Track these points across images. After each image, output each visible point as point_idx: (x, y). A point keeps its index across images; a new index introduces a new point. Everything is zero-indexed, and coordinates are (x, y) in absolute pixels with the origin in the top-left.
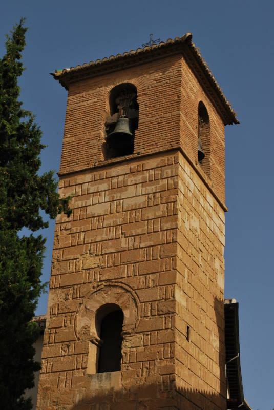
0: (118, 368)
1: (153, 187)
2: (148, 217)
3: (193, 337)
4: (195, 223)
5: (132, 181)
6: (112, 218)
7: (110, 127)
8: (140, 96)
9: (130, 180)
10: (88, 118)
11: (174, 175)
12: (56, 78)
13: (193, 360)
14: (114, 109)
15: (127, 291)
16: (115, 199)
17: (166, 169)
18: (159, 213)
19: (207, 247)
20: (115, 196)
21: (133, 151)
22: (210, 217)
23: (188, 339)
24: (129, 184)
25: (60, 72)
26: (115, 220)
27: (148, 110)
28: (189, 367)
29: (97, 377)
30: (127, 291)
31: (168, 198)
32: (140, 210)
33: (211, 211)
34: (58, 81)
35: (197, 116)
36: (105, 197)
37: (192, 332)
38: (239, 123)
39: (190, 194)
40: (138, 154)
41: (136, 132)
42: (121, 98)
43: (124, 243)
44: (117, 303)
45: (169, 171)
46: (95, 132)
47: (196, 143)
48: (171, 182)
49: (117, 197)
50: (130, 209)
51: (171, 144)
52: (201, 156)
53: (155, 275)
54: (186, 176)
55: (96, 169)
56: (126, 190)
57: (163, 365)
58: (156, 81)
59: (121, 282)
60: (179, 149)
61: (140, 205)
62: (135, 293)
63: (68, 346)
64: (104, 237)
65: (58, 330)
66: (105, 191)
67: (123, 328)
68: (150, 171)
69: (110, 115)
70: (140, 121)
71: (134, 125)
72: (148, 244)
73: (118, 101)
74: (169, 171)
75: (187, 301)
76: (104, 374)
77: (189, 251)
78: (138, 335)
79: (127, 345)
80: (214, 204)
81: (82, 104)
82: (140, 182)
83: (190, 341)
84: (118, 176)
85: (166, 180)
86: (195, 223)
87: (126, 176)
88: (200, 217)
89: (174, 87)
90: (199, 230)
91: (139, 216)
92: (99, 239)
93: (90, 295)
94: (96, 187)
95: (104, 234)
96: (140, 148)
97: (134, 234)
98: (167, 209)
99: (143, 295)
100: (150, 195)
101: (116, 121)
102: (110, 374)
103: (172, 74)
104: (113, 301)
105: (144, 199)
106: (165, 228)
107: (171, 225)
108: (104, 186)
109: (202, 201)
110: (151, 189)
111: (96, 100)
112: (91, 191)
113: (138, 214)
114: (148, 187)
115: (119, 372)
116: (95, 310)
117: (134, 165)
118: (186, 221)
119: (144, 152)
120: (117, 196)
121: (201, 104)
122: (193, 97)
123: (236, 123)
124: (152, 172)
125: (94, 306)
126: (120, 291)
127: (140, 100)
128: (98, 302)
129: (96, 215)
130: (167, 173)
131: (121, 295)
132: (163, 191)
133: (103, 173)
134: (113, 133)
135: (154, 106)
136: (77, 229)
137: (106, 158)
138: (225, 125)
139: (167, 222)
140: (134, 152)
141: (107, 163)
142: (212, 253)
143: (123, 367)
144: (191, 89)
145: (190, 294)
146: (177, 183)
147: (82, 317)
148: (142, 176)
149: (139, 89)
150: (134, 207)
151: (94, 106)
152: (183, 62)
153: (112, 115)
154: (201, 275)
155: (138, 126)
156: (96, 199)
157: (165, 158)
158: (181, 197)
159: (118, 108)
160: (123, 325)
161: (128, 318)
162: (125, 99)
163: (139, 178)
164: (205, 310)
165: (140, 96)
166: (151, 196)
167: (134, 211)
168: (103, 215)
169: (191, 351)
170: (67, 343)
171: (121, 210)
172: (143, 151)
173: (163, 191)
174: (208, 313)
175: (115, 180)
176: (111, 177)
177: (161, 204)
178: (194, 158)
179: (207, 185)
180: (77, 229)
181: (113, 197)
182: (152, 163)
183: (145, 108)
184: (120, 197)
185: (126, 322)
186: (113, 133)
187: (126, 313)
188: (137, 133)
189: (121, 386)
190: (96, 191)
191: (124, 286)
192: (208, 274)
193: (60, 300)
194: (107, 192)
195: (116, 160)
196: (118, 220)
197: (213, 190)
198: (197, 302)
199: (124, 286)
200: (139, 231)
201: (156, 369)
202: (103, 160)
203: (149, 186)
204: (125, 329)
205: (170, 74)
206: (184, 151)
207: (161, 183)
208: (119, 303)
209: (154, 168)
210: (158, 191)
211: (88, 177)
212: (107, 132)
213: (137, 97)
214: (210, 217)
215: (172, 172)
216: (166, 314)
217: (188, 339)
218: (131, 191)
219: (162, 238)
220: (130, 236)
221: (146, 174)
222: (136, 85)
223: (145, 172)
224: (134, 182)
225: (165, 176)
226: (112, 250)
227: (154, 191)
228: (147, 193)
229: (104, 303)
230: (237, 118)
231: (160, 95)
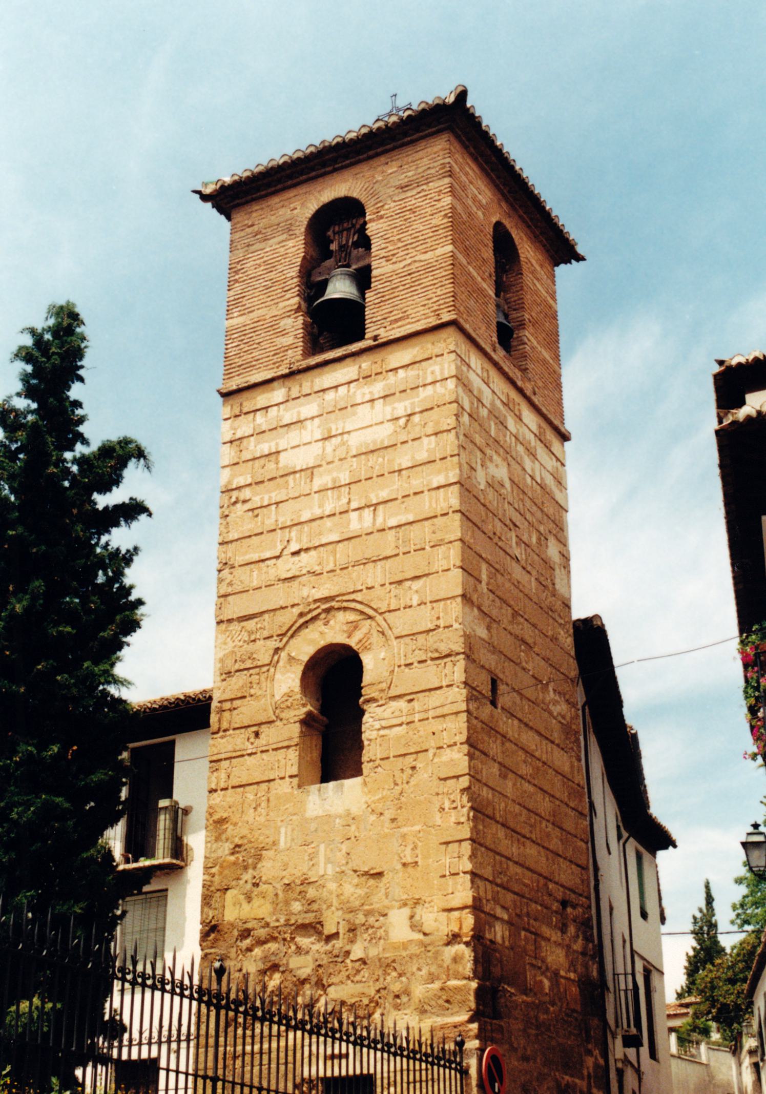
0: (357, 771)
1: (407, 403)
2: (400, 464)
3: (505, 699)
4: (500, 471)
9: (362, 392)
10: (272, 275)
12: (204, 198)
13: (508, 744)
15: (370, 617)
16: (333, 433)
17: (431, 365)
18: (423, 456)
19: (528, 516)
20: (334, 427)
21: (365, 334)
22: (533, 455)
23: (494, 703)
24: (359, 401)
26: (335, 475)
27: (391, 248)
28: (499, 760)
29: (317, 792)
30: (370, 617)
31: (437, 423)
33: (533, 444)
35: (491, 252)
36: (313, 430)
37: (502, 688)
39: (484, 412)
40: (375, 338)
41: (367, 296)
42: (337, 228)
43: (357, 523)
45: (437, 368)
46: (287, 303)
47: (492, 308)
49: (337, 429)
51: (438, 315)
52: (506, 335)
54: (472, 376)
55: (291, 374)
56: (354, 414)
58: (402, 188)
59: (354, 601)
61: (382, 441)
63: (257, 735)
64: (318, 512)
65: (237, 703)
66: (312, 418)
67: (363, 692)
70: (374, 273)
71: (363, 279)
72: (403, 519)
75: (489, 628)
76: (332, 784)
77: (489, 528)
78: (394, 704)
79: (373, 723)
80: (540, 427)
83: (499, 706)
86: (500, 471)
88: (507, 454)
89: (437, 198)
90: (508, 484)
92: (306, 516)
93: (293, 632)
96: (377, 326)
97: (374, 502)
102: (342, 785)
103: (433, 171)
104: (341, 639)
105: (389, 428)
107: (447, 477)
108: (309, 408)
109: (511, 423)
110: (401, 407)
112: (286, 421)
114: (396, 405)
115: (358, 780)
116: (306, 658)
117: (366, 363)
118: (479, 467)
119: (385, 334)
122: (480, 214)
126: (352, 617)
128: (311, 642)
129: (298, 468)
130: (432, 373)
135: (399, 240)
136: (262, 499)
140: (366, 337)
141: (313, 361)
142: (542, 529)
143: (366, 768)
144: (475, 199)
145: (494, 613)
148: (384, 382)
151: (282, 249)
154: (517, 572)
155: (370, 283)
156: (293, 436)
160: (362, 685)
163: (378, 388)
164: (530, 641)
165: (372, 220)
169: (502, 728)
170: (255, 729)
174: (536, 649)
175: (330, 396)
178: (488, 337)
179: (520, 391)
181: (330, 430)
182: (399, 356)
183: (383, 246)
184: (343, 428)
185: (367, 679)
187: (367, 660)
190: (294, 420)
191: (359, 607)
192: (534, 573)
193: (237, 643)
194: (317, 420)
196: (341, 476)
197: (535, 399)
198: (510, 628)
199: (359, 607)
200: (384, 494)
203: (400, 400)
205: (429, 172)
206: (467, 326)
208: (353, 643)
209: (407, 366)
210: (417, 410)
211: (278, 394)
213: (365, 223)
214: (533, 455)
215: (442, 370)
218: (365, 414)
220: (369, 506)
226: (335, 537)
227: (409, 412)
230: (580, 249)
231: (412, 215)
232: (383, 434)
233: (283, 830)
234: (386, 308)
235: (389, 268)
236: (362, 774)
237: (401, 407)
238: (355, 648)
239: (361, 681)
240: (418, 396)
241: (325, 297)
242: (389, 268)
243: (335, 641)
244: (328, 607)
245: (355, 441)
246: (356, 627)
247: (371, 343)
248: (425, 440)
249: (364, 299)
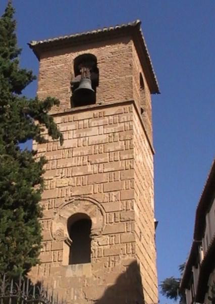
0: (89, 261)
1: (113, 128)
5: (95, 124)
6: (80, 150)
7: (75, 86)
8: (99, 63)
9: (94, 123)
11: (129, 120)
12: (31, 47)
14: (77, 72)
16: (81, 136)
18: (119, 148)
20: (82, 134)
24: (93, 125)
25: (34, 43)
26: (82, 151)
29: (71, 268)
30: (95, 204)
31: (125, 137)
32: (103, 145)
34: (32, 50)
40: (100, 104)
43: (90, 169)
44: (86, 213)
48: (127, 125)
50: (94, 143)
53: (117, 192)
56: (91, 130)
57: (126, 259)
59: (89, 198)
60: (132, 102)
61: (102, 141)
62: (101, 205)
64: (74, 164)
66: (73, 130)
67: (92, 231)
68: (110, 117)
69: (74, 76)
70: (100, 81)
71: (95, 83)
73: (79, 66)
74: (125, 117)
81: (51, 67)
82: (102, 124)
84: (83, 120)
85: (123, 124)
87: (90, 120)
91: (101, 149)
94: (65, 127)
95: (74, 161)
96: (100, 99)
97: (98, 162)
98: (125, 144)
99: (108, 207)
100: (110, 135)
101: (79, 81)
102: (82, 266)
104: (83, 211)
106: (124, 158)
107: (128, 156)
108: (72, 126)
110: (110, 130)
111: (63, 65)
113: (101, 148)
114: (108, 129)
115: (89, 264)
116: (67, 217)
117: (96, 112)
119: (104, 103)
121: (141, 74)
123: (158, 93)
124: (111, 118)
125: (67, 214)
126: (88, 203)
127: (99, 66)
128: (70, 211)
130: (124, 118)
131: (89, 207)
132: (121, 131)
133: (71, 116)
134: (78, 88)
136: (50, 157)
137: (72, 107)
138: (151, 93)
139: (125, 154)
141: (74, 109)
146: (132, 126)
147: (57, 223)
148: (104, 120)
149: (98, 58)
150: (97, 143)
152: (132, 42)
153: (75, 77)
155: (98, 84)
157: (121, 108)
158: (134, 136)
159: (81, 71)
160: (92, 229)
161: (96, 224)
162: (87, 64)
163: (101, 122)
165: (99, 63)
166: (110, 135)
167: (97, 146)
168: (72, 148)
171: (87, 145)
172: (103, 102)
173: (121, 131)
175: (81, 123)
176: (78, 120)
177: (120, 140)
180: (50, 157)
181: (80, 135)
182: (109, 111)
185: (93, 227)
186: (78, 88)
187: (94, 220)
189: (91, 274)
191: (91, 200)
194: (75, 131)
195: (82, 108)
199: (91, 200)
200: (103, 160)
201: (120, 262)
202: (70, 108)
203: (109, 127)
204: (93, 232)
207: (119, 125)
208: (88, 213)
209: (113, 115)
212: (72, 89)
215: (127, 118)
216: (128, 221)
217: (140, 240)
218: (95, 131)
219: (122, 166)
220: (95, 164)
221: (107, 119)
222: (96, 55)
223: (106, 117)
224: (96, 125)
225: (122, 121)
226: (81, 174)
228: (108, 132)
229: (75, 212)
232: (104, 138)
233: (55, 282)
234: (105, 93)
235: (106, 80)
236: (89, 261)
237: (110, 130)
238: (89, 215)
239: (91, 227)
240: (117, 125)
242: (106, 80)
243: (80, 212)
244: (80, 198)
245: (92, 140)
246: (89, 207)
247: (98, 105)
249: (95, 90)
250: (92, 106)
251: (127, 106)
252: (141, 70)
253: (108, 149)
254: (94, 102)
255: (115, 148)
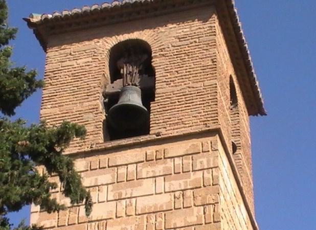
1: (181, 182)
2: (175, 224)
5: (148, 172)
6: (120, 224)
7: (111, 99)
8: (156, 57)
9: (146, 171)
10: (79, 83)
11: (212, 166)
12: (30, 24)
14: (115, 74)
16: (123, 196)
17: (200, 158)
18: (193, 219)
20: (123, 192)
21: (149, 131)
25: (37, 18)
27: (169, 76)
31: (204, 198)
32: (163, 213)
38: (266, 115)
40: (158, 134)
41: (151, 105)
46: (90, 103)
48: (208, 175)
49: (126, 194)
50: (147, 211)
51: (206, 124)
58: (179, 39)
60: (217, 132)
61: (162, 206)
66: (107, 184)
68: (176, 159)
69: (110, 82)
70: (157, 91)
71: (149, 95)
74: (205, 160)
81: (68, 63)
82: (161, 174)
84: (127, 165)
85: (201, 172)
87: (139, 165)
89: (205, 48)
91: (161, 222)
94: (93, 178)
96: (158, 125)
98: (204, 213)
100: (177, 194)
101: (120, 90)
103: (202, 30)
108: (105, 178)
110: (177, 184)
111: (90, 59)
113: (159, 219)
114: (173, 182)
117: (151, 150)
119: (165, 133)
120: (126, 192)
121: (231, 77)
127: (156, 62)
130: (201, 163)
132: (196, 188)
133: (104, 158)
134: (116, 105)
135: (177, 72)
137: (106, 140)
140: (150, 133)
146: (218, 177)
148: (164, 165)
149: (154, 48)
150: (153, 210)
151: (87, 67)
152: (215, 17)
153: (112, 82)
155: (155, 97)
158: (222, 198)
159: (122, 72)
162: (133, 59)
163: (159, 169)
165: (156, 57)
166: (177, 194)
167: (153, 215)
168: (106, 219)
171: (133, 213)
172: (163, 131)
173: (196, 188)
175: (122, 170)
176: (117, 166)
177: (195, 205)
181: (120, 194)
183: (165, 74)
184: (131, 194)
186: (116, 105)
188: (153, 105)
190: (93, 185)
202: (101, 141)
205: (199, 30)
207: (193, 176)
210: (189, 187)
212: (107, 106)
215: (208, 162)
218: (148, 186)
221: (170, 163)
223: (169, 160)
224: (151, 174)
225: (198, 167)
227: (183, 188)
228: (172, 190)
231: (187, 57)
232: (164, 200)
234: (167, 115)
235: (168, 89)
237: (177, 184)
240: (189, 177)
241: (119, 103)
242: (168, 89)
247: (154, 137)
248: (196, 209)
249: (149, 108)
250: (143, 139)
251: (208, 140)
252: (230, 71)
253: (173, 222)
254: (146, 131)
255: (185, 220)
